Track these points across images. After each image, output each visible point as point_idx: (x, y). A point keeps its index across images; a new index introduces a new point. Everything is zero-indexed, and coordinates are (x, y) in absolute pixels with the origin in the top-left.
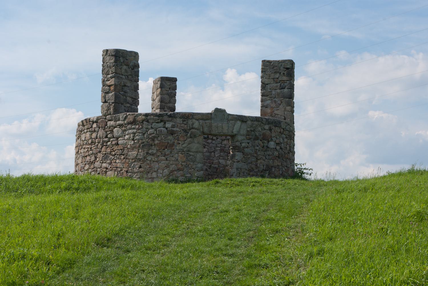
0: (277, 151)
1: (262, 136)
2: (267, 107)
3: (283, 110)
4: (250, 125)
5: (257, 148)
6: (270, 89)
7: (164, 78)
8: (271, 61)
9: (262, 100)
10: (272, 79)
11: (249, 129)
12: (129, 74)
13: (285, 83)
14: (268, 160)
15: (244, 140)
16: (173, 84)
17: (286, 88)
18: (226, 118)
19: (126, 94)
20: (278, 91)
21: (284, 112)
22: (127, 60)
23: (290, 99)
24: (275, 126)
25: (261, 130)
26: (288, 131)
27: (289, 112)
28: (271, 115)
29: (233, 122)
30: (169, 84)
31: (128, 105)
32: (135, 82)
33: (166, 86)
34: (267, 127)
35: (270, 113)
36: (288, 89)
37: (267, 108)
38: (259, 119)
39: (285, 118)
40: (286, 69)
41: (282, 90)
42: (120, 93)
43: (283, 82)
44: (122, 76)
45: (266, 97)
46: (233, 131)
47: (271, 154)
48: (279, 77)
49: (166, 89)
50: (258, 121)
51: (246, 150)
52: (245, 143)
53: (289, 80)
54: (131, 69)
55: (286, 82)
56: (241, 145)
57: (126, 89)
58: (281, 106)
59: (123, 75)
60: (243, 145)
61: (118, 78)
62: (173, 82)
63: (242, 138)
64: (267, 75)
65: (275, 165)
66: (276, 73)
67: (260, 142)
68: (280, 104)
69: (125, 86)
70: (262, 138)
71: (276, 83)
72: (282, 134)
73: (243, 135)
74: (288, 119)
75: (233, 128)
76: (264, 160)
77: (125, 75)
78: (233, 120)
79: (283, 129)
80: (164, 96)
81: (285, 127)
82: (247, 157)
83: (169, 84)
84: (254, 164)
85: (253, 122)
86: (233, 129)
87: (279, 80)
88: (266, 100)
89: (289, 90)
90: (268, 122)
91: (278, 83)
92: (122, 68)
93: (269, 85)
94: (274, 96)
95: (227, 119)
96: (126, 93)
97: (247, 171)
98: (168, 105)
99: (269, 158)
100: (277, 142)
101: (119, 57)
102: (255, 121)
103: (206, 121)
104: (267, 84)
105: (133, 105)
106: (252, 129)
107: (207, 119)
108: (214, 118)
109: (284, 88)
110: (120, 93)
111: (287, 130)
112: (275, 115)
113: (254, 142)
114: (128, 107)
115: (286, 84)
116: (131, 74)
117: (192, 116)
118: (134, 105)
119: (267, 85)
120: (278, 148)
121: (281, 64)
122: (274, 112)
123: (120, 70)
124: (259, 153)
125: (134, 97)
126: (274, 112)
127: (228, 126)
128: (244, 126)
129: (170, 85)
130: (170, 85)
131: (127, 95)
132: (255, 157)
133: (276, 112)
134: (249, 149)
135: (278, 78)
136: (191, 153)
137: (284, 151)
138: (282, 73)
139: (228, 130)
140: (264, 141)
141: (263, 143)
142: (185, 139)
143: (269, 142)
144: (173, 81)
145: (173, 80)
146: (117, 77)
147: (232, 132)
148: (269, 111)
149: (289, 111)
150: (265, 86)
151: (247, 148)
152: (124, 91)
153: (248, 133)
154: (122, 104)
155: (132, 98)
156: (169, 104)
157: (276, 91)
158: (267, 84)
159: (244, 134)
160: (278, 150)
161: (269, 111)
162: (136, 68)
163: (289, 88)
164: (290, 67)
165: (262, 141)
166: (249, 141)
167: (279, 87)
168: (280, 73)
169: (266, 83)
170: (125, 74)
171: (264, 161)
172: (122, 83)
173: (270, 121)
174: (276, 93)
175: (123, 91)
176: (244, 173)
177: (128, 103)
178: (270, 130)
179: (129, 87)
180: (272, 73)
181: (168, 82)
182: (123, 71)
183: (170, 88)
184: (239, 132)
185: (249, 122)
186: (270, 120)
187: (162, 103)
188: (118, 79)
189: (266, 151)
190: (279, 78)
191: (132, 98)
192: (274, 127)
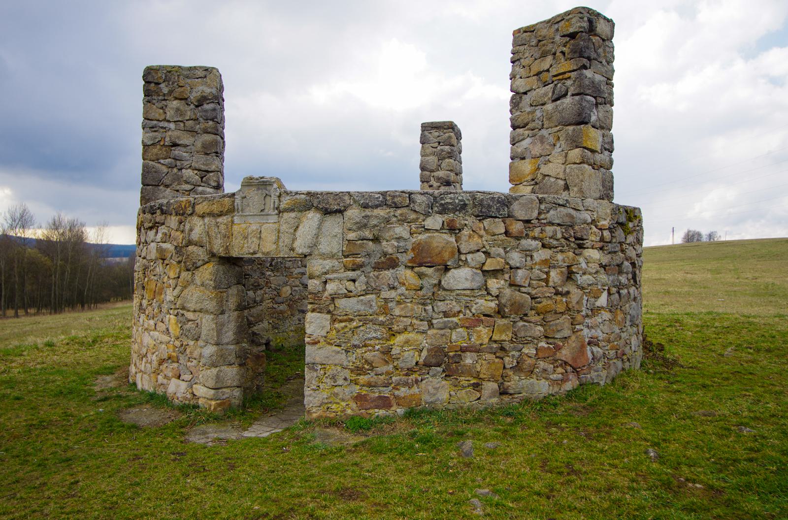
0: (489, 298)
1: (411, 255)
2: (524, 158)
3: (561, 160)
4: (357, 223)
5: (393, 294)
6: (531, 105)
7: (426, 125)
8: (533, 26)
9: (514, 140)
10: (534, 75)
11: (352, 236)
12: (188, 118)
13: (566, 79)
14: (442, 332)
15: (334, 272)
17: (569, 94)
18: (272, 206)
19: (178, 163)
20: (550, 107)
21: (563, 166)
22: (182, 87)
23: (578, 127)
24: (477, 216)
25: (406, 235)
26: (559, 225)
27: (575, 166)
28: (533, 180)
29: (293, 215)
30: (437, 134)
31: (188, 187)
34: (435, 221)
35: (530, 174)
36: (573, 95)
37: (523, 161)
38: (396, 200)
39: (566, 184)
40: (568, 39)
41: (558, 102)
42: (162, 161)
43: (561, 77)
44: (166, 124)
45: (522, 129)
46: (294, 246)
47: (457, 309)
48: (551, 66)
49: (431, 145)
50: (390, 206)
51: (341, 303)
52: (340, 280)
53: (575, 68)
54: (192, 106)
55: (569, 78)
56: (324, 290)
57: (177, 152)
58: (557, 149)
59: (169, 121)
60: (331, 287)
61: (153, 130)
62: (445, 131)
63: (328, 264)
64: (524, 67)
65: (478, 343)
66: (544, 55)
67: (407, 275)
68: (554, 145)
69: (175, 145)
70: (412, 260)
71: (545, 86)
72: (518, 238)
73: (332, 256)
74: (575, 186)
75: (295, 235)
76: (424, 332)
77: (175, 122)
78: (292, 210)
79: (528, 222)
80: (428, 158)
81: (535, 214)
82: (346, 326)
83: (437, 134)
84: (377, 347)
85: (368, 212)
86: (294, 240)
87: (551, 74)
88: (521, 138)
89: (577, 98)
90: (442, 205)
91: (549, 84)
93: (529, 93)
94: (540, 123)
97: (347, 373)
98: (436, 174)
99: (445, 322)
100: (485, 268)
101: (157, 84)
102: (377, 207)
103: (218, 220)
104: (525, 93)
105: (201, 186)
106: (367, 234)
107: (221, 215)
108: (240, 208)
109: (565, 95)
111: (551, 224)
112: (543, 179)
113: (377, 277)
114: (186, 191)
115: (569, 83)
116: (193, 117)
117: (193, 207)
118: (203, 184)
119: (524, 97)
120: (494, 284)
121: (556, 26)
122: (538, 169)
123: (161, 111)
124: (397, 311)
125: (203, 167)
126: (541, 171)
127: (279, 232)
128: (333, 225)
129: (438, 136)
130: (438, 136)
131: (182, 164)
132: (382, 324)
133: (544, 170)
134: (353, 300)
135: (548, 71)
136: (190, 315)
137: (529, 294)
138: (558, 54)
139: (276, 242)
140: (423, 269)
141: (421, 276)
142: (177, 276)
143: (447, 269)
144: (445, 129)
146: (150, 128)
147: (292, 249)
148: (527, 167)
149: (575, 163)
150: (521, 98)
151: (346, 296)
152: (171, 156)
153: (350, 251)
154: (167, 186)
155: (199, 170)
156: (438, 172)
157: (544, 107)
158: (525, 93)
159: (335, 251)
160: (494, 292)
161: (527, 167)
162: (208, 101)
163: (576, 92)
164: (576, 30)
165: (416, 269)
166: (351, 274)
167: (550, 94)
168: (554, 54)
169: (522, 91)
170: (176, 119)
171: (420, 337)
172: (167, 139)
173: (449, 201)
174: (544, 114)
175: (170, 158)
176: (334, 378)
177: (187, 182)
178: (452, 229)
179: (188, 146)
180: (536, 59)
182: (170, 114)
183: (439, 143)
184: (314, 246)
185: (354, 213)
186: (451, 198)
187: (425, 172)
188: (155, 131)
189: (434, 298)
190: (550, 69)
191: (199, 170)
192: (470, 221)
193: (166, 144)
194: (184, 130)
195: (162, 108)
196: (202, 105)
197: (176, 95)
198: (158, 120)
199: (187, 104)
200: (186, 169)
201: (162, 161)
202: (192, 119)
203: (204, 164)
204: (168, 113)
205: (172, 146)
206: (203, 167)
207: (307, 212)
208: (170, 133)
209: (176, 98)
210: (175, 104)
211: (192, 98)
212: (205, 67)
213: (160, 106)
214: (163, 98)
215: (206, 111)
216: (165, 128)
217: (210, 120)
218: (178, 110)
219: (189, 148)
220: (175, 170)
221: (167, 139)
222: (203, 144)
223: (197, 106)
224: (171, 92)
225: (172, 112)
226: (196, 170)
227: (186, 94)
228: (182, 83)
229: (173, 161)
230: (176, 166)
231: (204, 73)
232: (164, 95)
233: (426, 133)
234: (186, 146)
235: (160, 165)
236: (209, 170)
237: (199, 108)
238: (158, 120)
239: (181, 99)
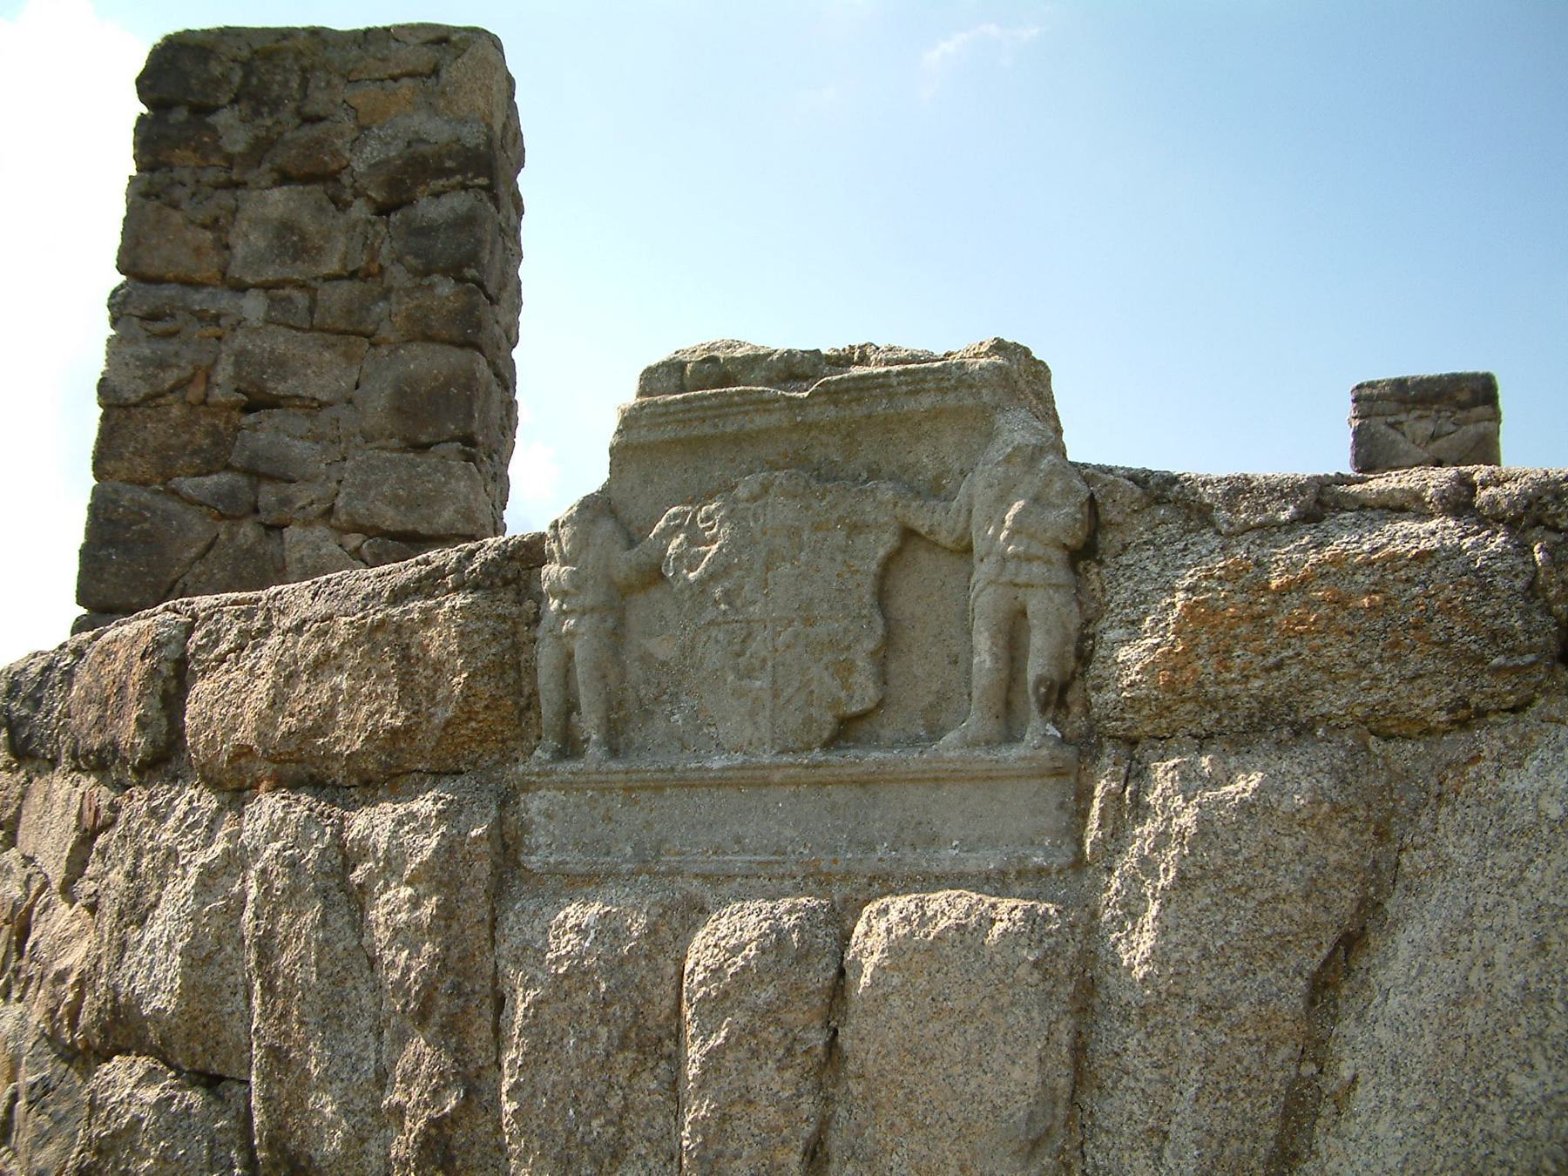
12: (333, 265)
16: (1458, 424)
19: (268, 495)
22: (319, 119)
30: (1426, 427)
32: (416, 348)
33: (1404, 445)
42: (187, 485)
44: (226, 302)
61: (159, 327)
62: (1460, 415)
69: (258, 402)
77: (266, 287)
83: (1426, 427)
92: (235, 212)
95: (1057, 697)
96: (271, 478)
103: (359, 822)
108: (589, 724)
110: (175, 493)
116: (360, 260)
123: (209, 235)
129: (1434, 437)
130: (1434, 437)
131: (285, 502)
144: (1463, 406)
145: (1463, 397)
152: (237, 459)
170: (270, 274)
172: (224, 372)
175: (228, 467)
181: (1420, 418)
182: (249, 241)
193: (218, 395)
194: (312, 329)
195: (213, 225)
196: (410, 202)
197: (284, 157)
198: (188, 283)
199: (335, 200)
200: (307, 524)
201: (187, 485)
202: (353, 275)
203: (395, 501)
204: (240, 250)
205: (248, 409)
206: (391, 512)
207: (1489, 741)
208: (240, 340)
209: (284, 178)
210: (278, 201)
211: (360, 167)
212: (438, 27)
213: (200, 217)
214: (223, 177)
215: (427, 231)
216: (216, 318)
217: (445, 273)
218: (286, 228)
219: (325, 415)
220: (248, 532)
221: (224, 372)
222: (399, 393)
223: (383, 210)
224: (261, 148)
225: (258, 240)
226: (358, 529)
227: (336, 154)
228: (318, 101)
229: (242, 481)
230: (256, 511)
231: (422, 58)
232: (230, 159)
233: (1378, 425)
234: (314, 406)
235: (174, 506)
236: (423, 529)
237: (395, 218)
238: (188, 283)
239: (308, 179)
